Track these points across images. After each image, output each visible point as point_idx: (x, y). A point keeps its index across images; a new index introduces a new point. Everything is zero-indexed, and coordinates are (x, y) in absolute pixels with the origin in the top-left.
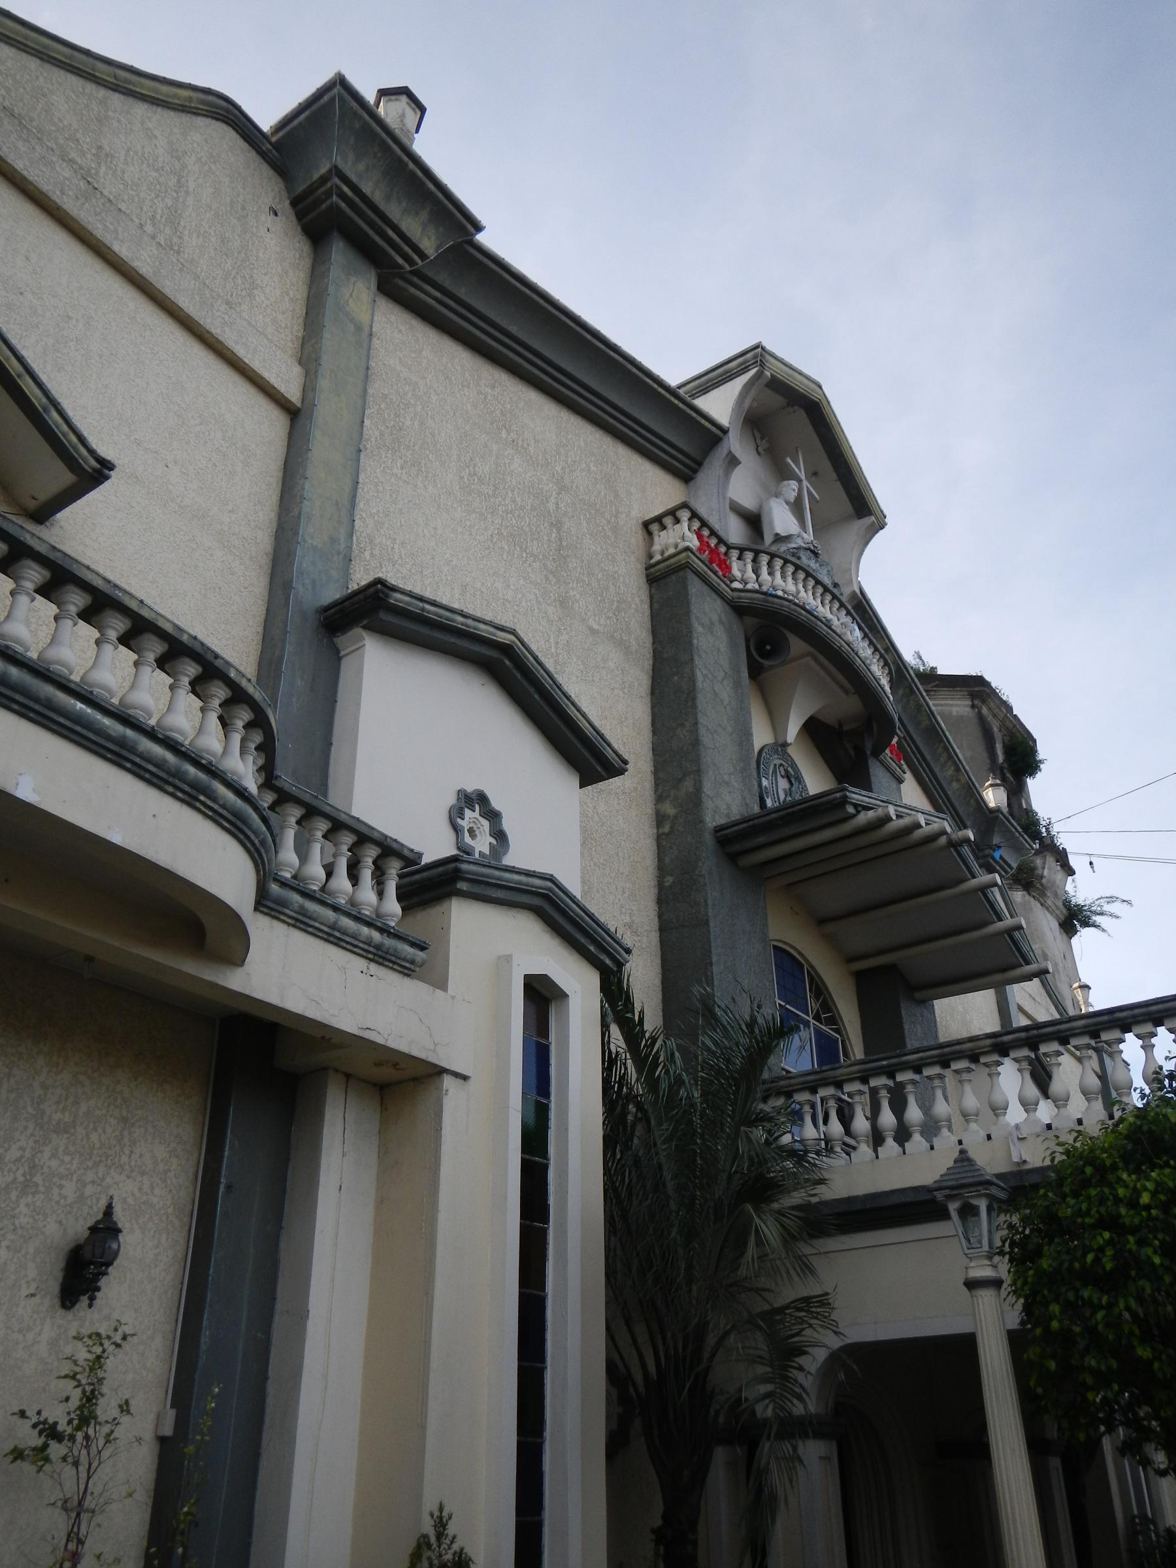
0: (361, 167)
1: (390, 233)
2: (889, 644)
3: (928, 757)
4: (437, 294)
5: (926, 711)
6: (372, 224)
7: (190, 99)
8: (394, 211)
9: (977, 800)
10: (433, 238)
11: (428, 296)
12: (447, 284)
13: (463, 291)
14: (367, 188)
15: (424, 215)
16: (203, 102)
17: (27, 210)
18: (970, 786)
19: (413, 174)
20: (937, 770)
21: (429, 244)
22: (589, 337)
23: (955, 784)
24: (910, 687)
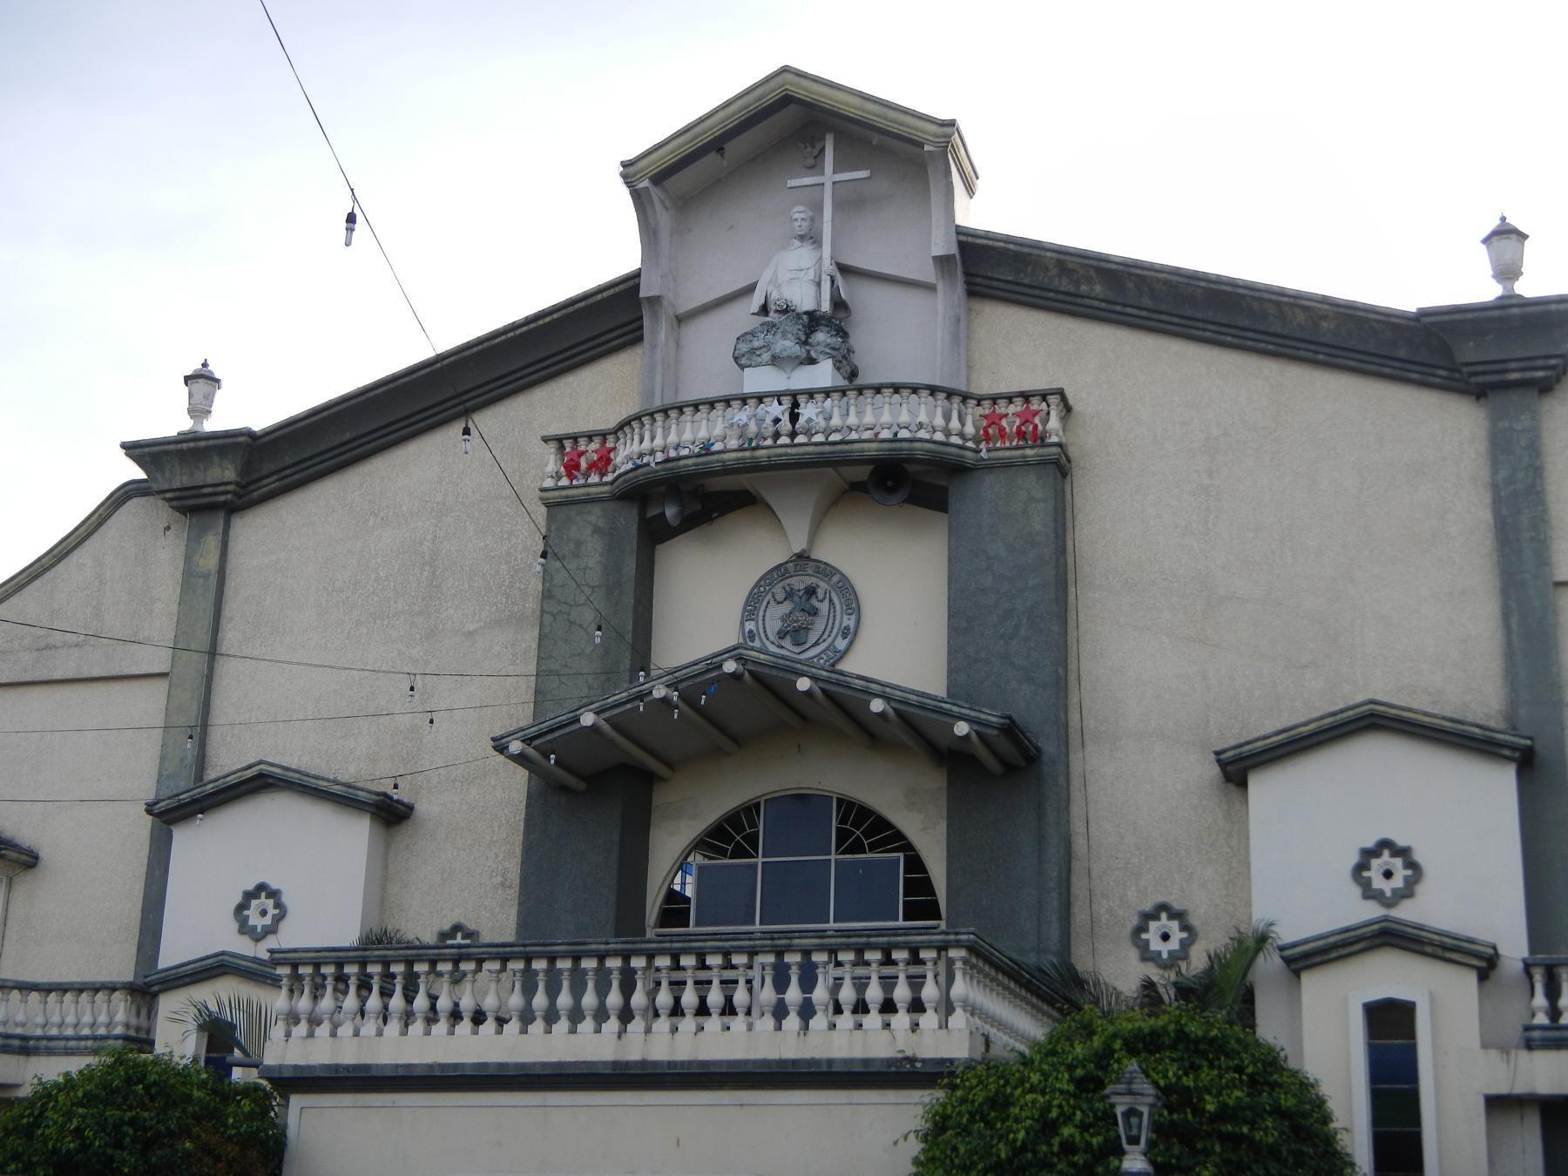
0: (167, 475)
1: (206, 491)
2: (1054, 255)
3: (1246, 323)
4: (275, 477)
5: (1181, 283)
6: (196, 497)
7: (100, 515)
8: (199, 478)
9: (1378, 321)
10: (230, 466)
11: (271, 484)
12: (272, 467)
13: (287, 458)
14: (176, 485)
15: (216, 459)
16: (106, 509)
17: (21, 690)
18: (1346, 315)
19: (190, 450)
20: (1277, 327)
21: (230, 474)
22: (406, 379)
23: (1324, 324)
24: (1131, 274)
